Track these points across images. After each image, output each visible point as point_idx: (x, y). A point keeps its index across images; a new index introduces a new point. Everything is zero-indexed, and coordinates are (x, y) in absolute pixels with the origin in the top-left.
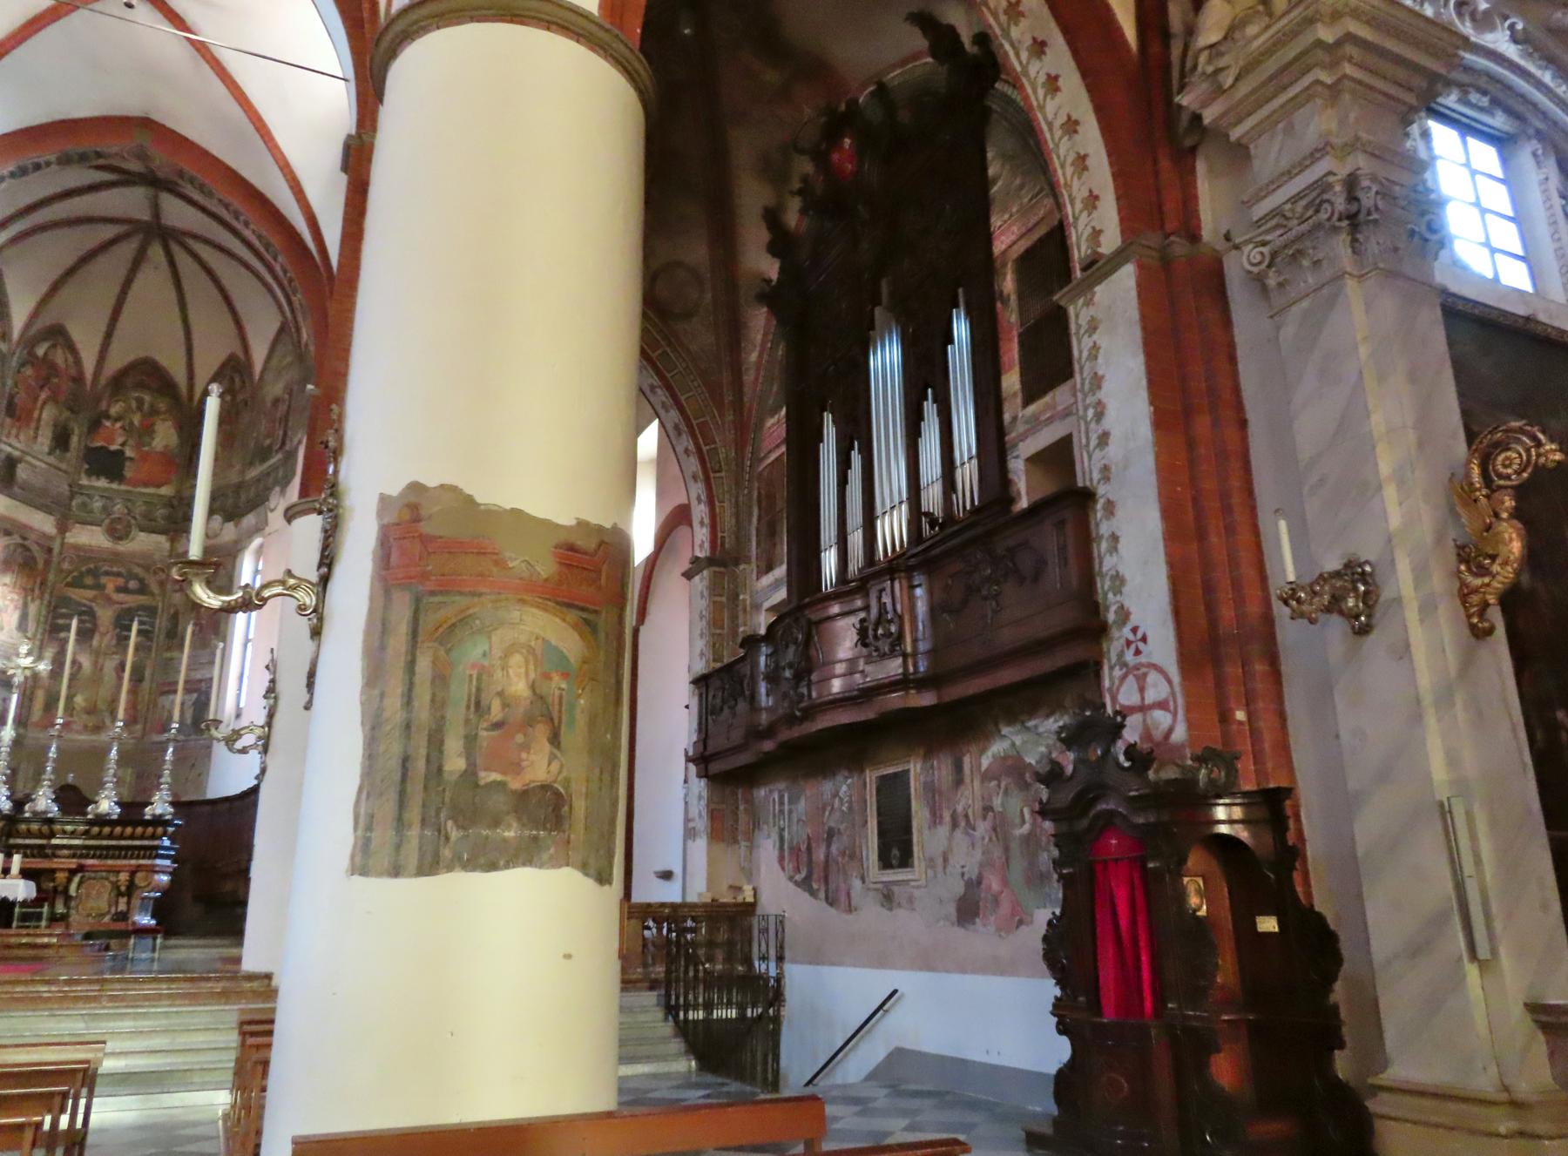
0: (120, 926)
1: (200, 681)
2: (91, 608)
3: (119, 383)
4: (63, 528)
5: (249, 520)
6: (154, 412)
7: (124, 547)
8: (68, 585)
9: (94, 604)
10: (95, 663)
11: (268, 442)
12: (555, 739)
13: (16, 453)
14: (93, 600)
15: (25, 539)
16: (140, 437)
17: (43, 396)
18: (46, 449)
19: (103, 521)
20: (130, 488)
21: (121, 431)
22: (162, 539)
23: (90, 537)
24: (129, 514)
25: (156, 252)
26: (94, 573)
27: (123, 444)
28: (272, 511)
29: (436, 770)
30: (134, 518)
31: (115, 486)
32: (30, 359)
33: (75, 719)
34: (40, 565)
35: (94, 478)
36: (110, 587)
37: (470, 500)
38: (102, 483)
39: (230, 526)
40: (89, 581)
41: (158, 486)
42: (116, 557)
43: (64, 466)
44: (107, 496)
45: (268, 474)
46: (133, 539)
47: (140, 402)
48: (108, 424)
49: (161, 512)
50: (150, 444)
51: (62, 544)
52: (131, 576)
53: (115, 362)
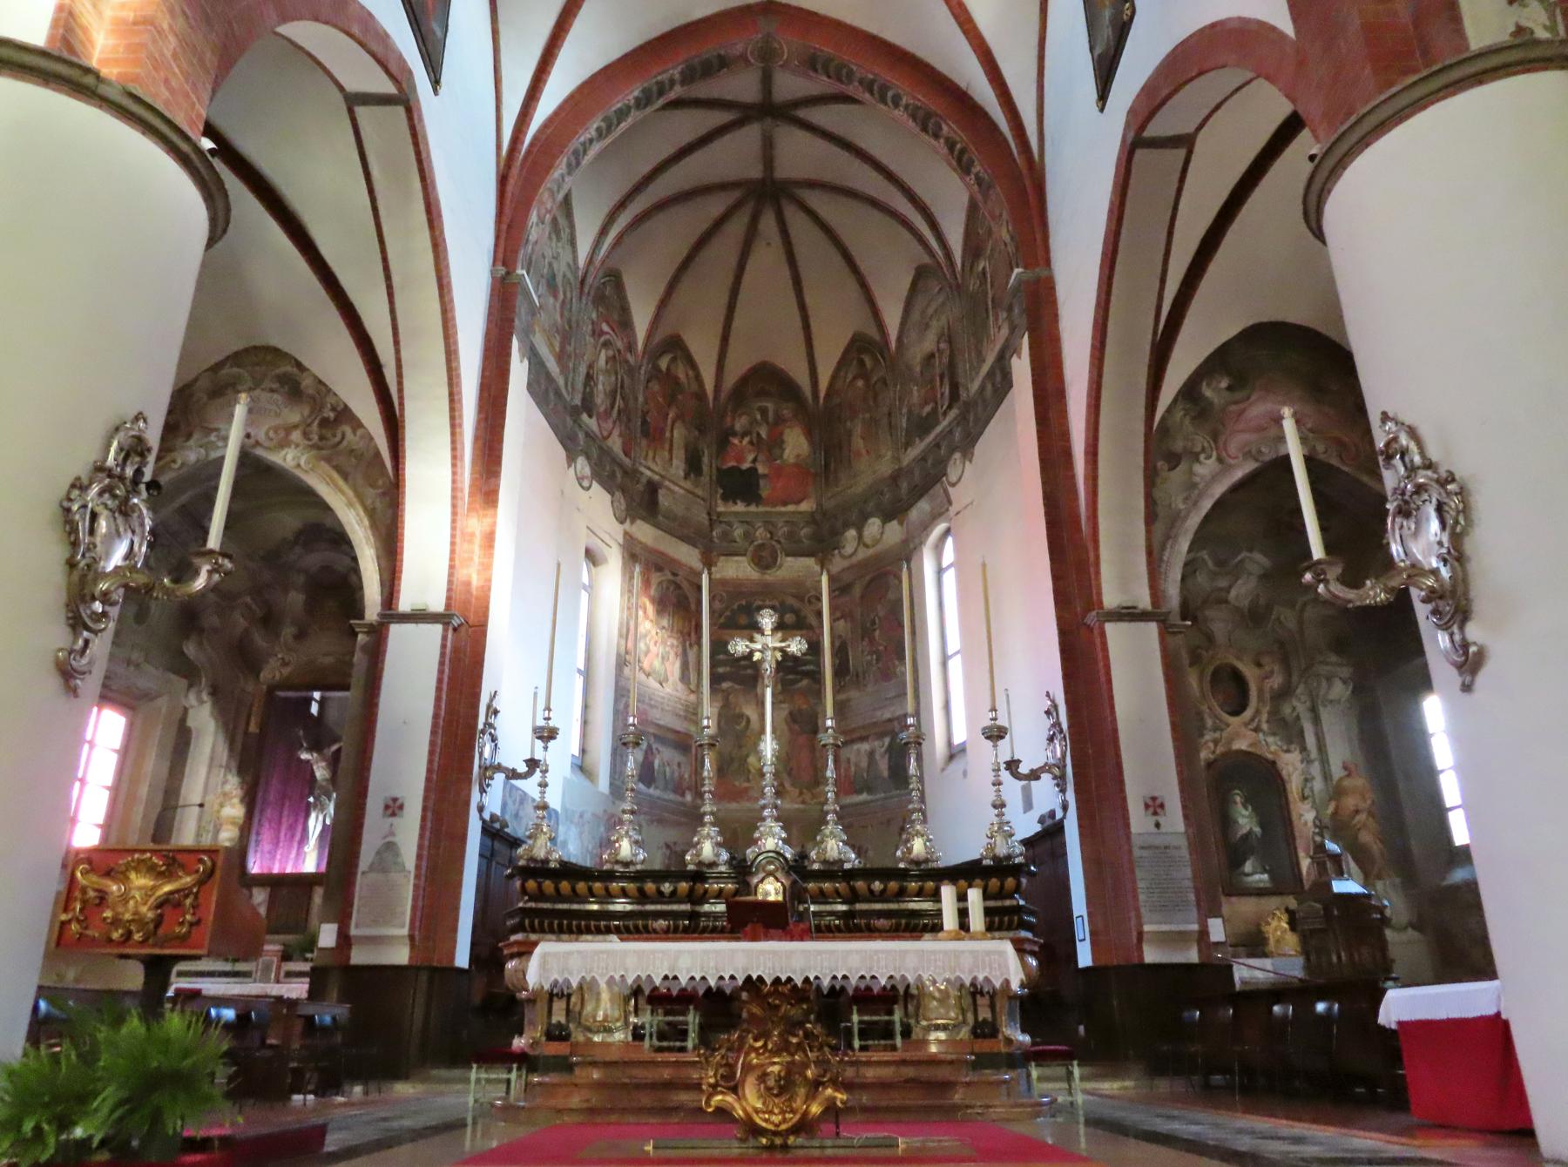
1: (890, 720)
6: (779, 421)
7: (773, 576)
11: (928, 409)
13: (656, 478)
15: (675, 575)
16: (770, 451)
18: (682, 473)
19: (746, 550)
20: (768, 509)
21: (750, 447)
24: (771, 538)
27: (755, 461)
28: (953, 485)
30: (779, 542)
31: (753, 508)
32: (655, 374)
35: (731, 503)
38: (740, 507)
41: (798, 502)
44: (746, 521)
45: (938, 446)
46: (780, 566)
47: (764, 411)
48: (736, 441)
49: (805, 532)
50: (781, 457)
53: (737, 367)
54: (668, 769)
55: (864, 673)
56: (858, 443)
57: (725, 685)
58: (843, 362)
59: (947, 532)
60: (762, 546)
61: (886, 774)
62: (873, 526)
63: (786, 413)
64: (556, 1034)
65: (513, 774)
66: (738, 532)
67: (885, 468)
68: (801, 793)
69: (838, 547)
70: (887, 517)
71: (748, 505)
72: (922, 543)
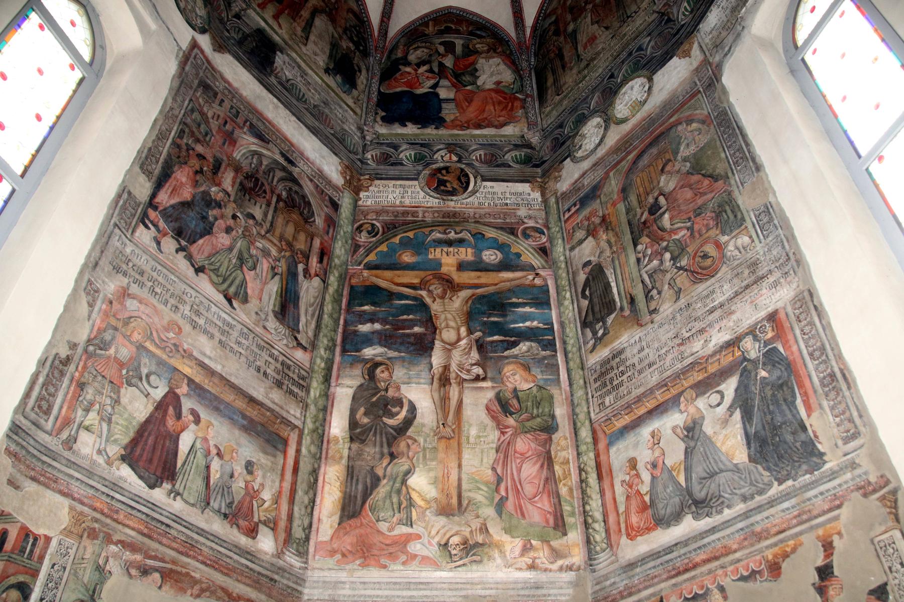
9: (424, 293)
10: (444, 400)
24: (459, 161)
27: (435, 86)
31: (430, 131)
33: (417, 529)
34: (319, 221)
35: (397, 125)
38: (411, 129)
40: (407, 258)
41: (502, 126)
42: (450, 220)
46: (474, 192)
50: (474, 83)
54: (216, 465)
55: (648, 297)
57: (369, 352)
61: (741, 456)
68: (527, 548)
71: (424, 127)
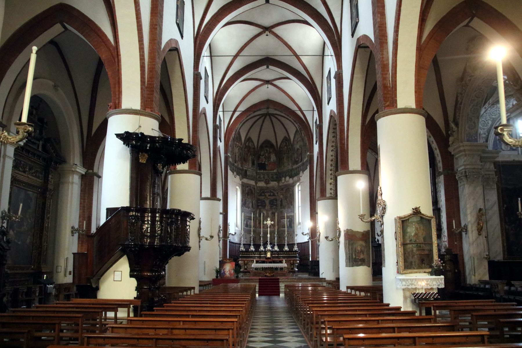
0: (292, 270)
1: (290, 216)
2: (264, 200)
3: (262, 147)
4: (256, 183)
5: (296, 178)
6: (270, 153)
7: (269, 185)
8: (259, 196)
10: (267, 212)
11: (297, 160)
12: (363, 254)
13: (246, 169)
14: (264, 199)
15: (250, 187)
17: (249, 154)
18: (251, 166)
20: (268, 171)
22: (276, 182)
23: (261, 184)
25: (268, 117)
26: (263, 192)
27: (265, 161)
28: (301, 177)
29: (352, 257)
31: (264, 172)
32: (246, 147)
36: (267, 195)
37: (353, 230)
38: (262, 171)
39: (291, 179)
40: (263, 194)
41: (274, 170)
42: (268, 188)
43: (255, 169)
45: (298, 167)
47: (267, 150)
48: (261, 157)
49: (275, 177)
51: (257, 186)
52: (271, 192)
53: (261, 142)
56: (285, 160)
58: (282, 142)
59: (299, 184)
60: (266, 179)
62: (287, 178)
63: (271, 151)
64: (245, 269)
65: (233, 235)
66: (262, 176)
67: (290, 167)
69: (281, 180)
70: (290, 177)
72: (295, 185)
